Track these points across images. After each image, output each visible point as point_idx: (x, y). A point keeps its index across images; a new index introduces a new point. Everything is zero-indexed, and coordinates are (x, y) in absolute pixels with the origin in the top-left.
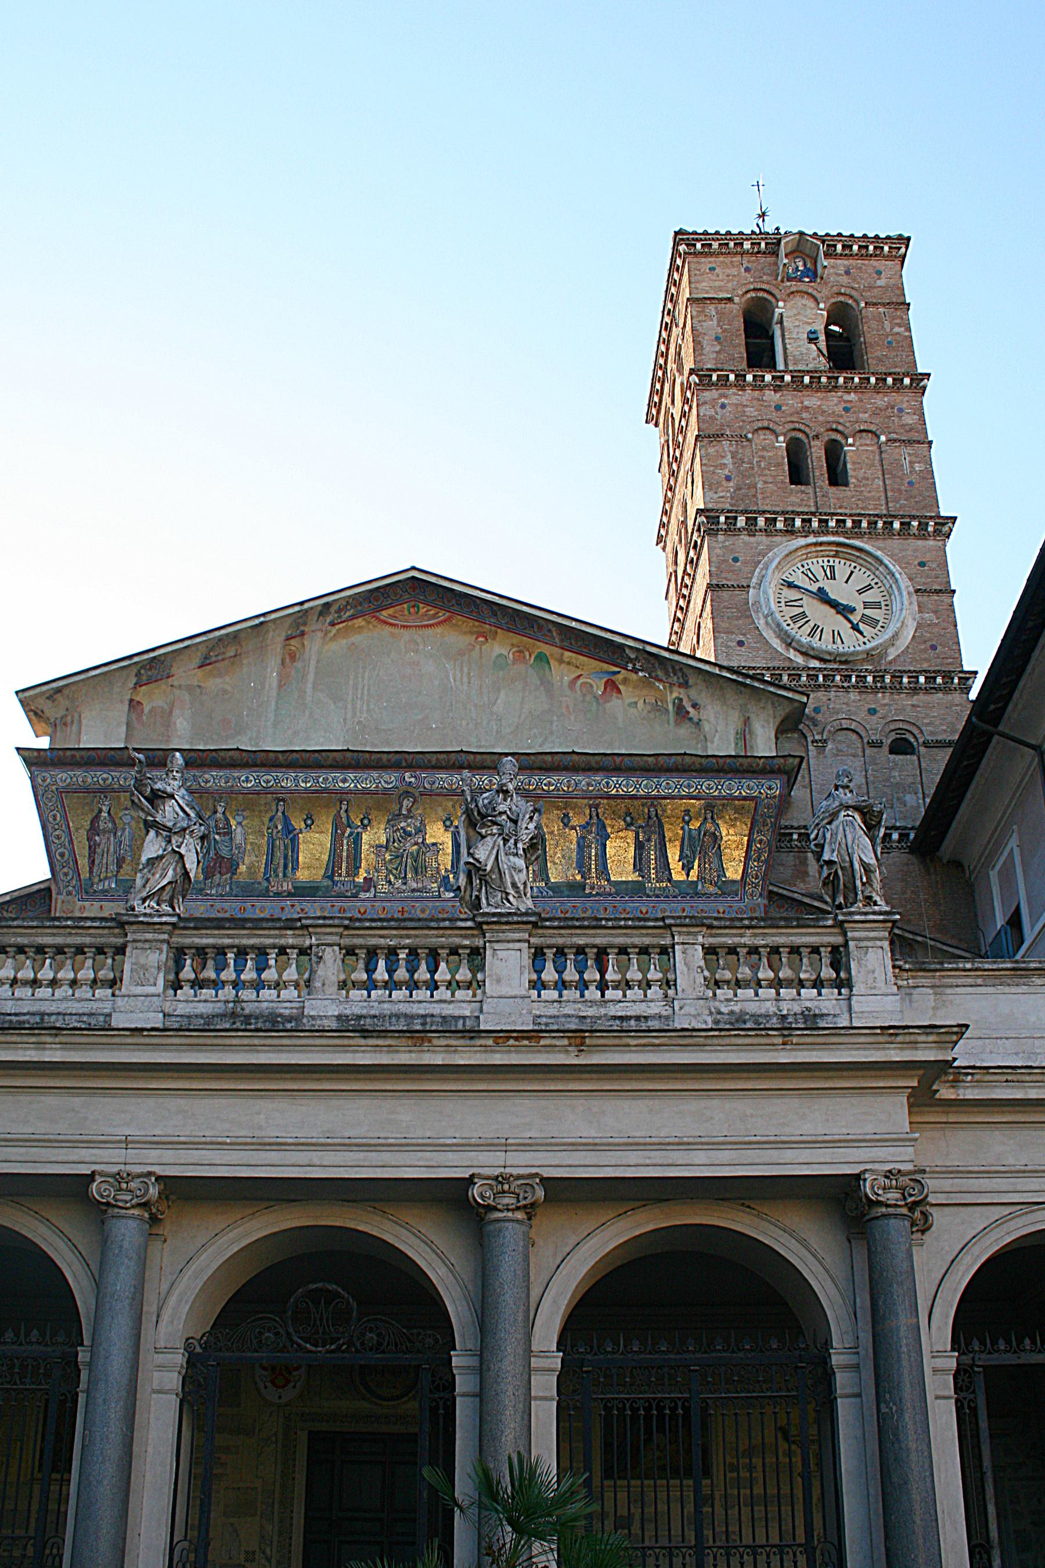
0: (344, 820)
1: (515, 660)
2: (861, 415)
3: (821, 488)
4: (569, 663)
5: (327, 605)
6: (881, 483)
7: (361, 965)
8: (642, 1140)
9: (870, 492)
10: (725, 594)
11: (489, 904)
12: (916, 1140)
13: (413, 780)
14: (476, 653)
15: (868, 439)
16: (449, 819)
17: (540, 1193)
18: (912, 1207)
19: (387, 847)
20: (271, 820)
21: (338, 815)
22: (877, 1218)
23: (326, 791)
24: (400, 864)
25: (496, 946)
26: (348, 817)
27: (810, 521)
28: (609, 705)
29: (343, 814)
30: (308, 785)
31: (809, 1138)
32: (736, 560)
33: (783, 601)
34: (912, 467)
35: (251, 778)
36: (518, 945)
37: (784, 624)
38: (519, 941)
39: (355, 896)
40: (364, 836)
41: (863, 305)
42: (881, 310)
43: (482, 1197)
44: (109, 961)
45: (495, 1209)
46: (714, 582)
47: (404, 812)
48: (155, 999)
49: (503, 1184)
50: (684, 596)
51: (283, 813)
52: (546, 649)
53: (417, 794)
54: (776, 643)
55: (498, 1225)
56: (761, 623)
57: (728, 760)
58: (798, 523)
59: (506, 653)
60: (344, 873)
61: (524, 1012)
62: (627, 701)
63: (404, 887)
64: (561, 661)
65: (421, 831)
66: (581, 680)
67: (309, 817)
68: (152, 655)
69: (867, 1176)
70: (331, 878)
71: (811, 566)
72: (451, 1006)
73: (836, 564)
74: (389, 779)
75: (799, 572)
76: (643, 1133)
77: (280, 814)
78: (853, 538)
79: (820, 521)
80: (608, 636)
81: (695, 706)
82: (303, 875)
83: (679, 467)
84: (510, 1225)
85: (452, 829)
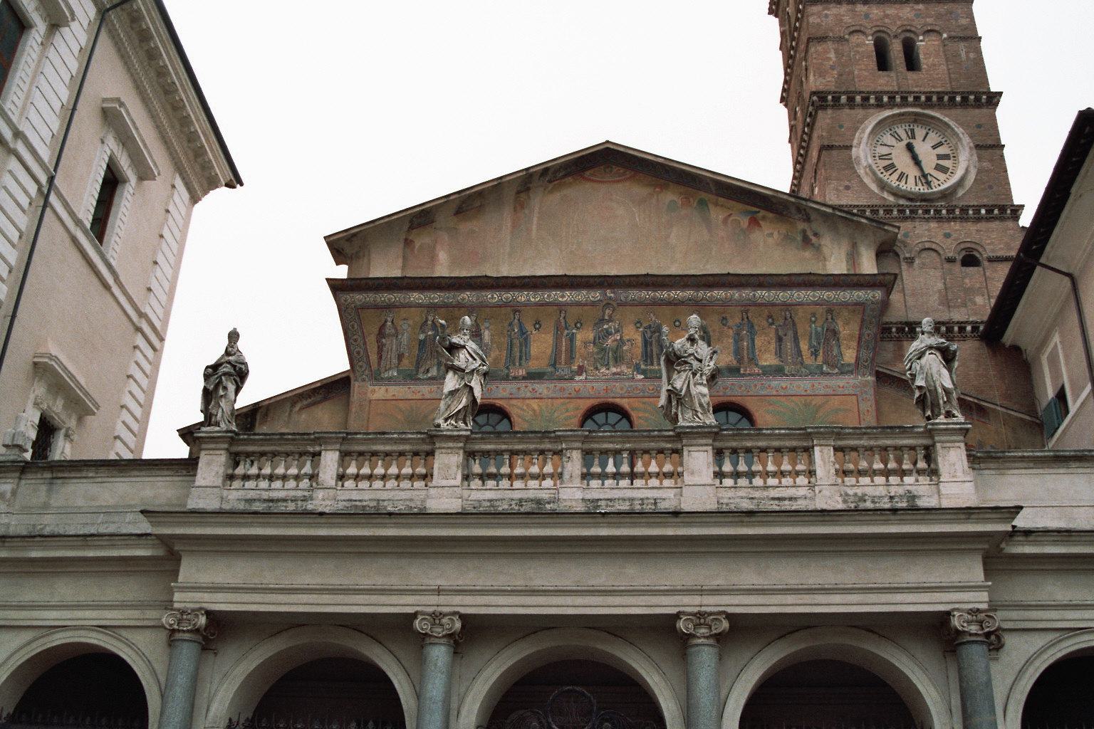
0: (563, 324)
1: (682, 204)
2: (928, 20)
3: (902, 73)
4: (722, 206)
7: (596, 462)
8: (796, 587)
9: (937, 74)
10: (834, 153)
11: (684, 419)
12: (989, 586)
13: (612, 295)
14: (654, 201)
15: (933, 37)
16: (638, 322)
17: (725, 625)
18: (988, 635)
19: (594, 343)
20: (510, 324)
21: (558, 322)
22: (964, 643)
23: (548, 304)
24: (604, 355)
25: (691, 448)
26: (566, 322)
27: (894, 97)
29: (563, 321)
30: (537, 300)
31: (913, 585)
32: (841, 126)
33: (877, 155)
35: (495, 296)
36: (705, 448)
37: (879, 173)
38: (706, 445)
39: (572, 379)
40: (579, 337)
43: (687, 629)
44: (423, 461)
46: (826, 143)
48: (456, 489)
49: (700, 618)
50: (803, 148)
51: (519, 320)
52: (704, 195)
53: (615, 305)
54: (874, 187)
55: (697, 648)
56: (861, 172)
57: (842, 278)
58: (885, 99)
59: (675, 199)
60: (563, 363)
61: (711, 495)
62: (766, 232)
63: (607, 372)
64: (716, 204)
65: (619, 331)
66: (731, 219)
67: (538, 322)
68: (423, 207)
69: (955, 613)
70: (554, 365)
71: (896, 129)
72: (661, 491)
73: (916, 128)
74: (596, 295)
75: (888, 135)
76: (798, 582)
77: (516, 321)
78: (927, 109)
79: (902, 98)
80: (752, 188)
81: (816, 234)
82: (534, 366)
83: (795, 52)
84: (706, 649)
85: (641, 329)
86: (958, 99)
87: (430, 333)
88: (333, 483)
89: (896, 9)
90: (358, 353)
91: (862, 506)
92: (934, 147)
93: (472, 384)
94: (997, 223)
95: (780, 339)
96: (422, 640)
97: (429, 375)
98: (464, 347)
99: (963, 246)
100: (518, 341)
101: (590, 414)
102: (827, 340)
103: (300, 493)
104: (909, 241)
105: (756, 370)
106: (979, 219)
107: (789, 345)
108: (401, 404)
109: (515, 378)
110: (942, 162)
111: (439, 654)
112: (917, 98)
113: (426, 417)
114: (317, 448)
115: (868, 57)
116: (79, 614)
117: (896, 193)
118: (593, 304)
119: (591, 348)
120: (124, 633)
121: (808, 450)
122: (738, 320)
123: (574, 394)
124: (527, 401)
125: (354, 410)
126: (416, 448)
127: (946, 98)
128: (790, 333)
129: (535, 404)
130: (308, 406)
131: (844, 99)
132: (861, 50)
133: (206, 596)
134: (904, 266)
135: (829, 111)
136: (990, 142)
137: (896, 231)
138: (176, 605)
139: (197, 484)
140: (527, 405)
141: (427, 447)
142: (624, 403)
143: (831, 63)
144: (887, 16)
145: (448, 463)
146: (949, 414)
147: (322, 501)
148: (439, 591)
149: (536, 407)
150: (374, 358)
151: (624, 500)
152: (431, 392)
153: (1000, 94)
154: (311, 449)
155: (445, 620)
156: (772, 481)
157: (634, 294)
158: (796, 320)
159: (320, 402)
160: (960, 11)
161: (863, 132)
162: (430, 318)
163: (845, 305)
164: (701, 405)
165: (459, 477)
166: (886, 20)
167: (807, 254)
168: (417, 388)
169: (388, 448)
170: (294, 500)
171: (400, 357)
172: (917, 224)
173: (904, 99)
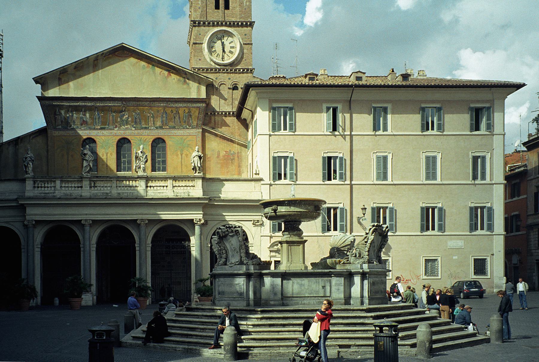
5: (103, 53)
17: (147, 222)
28: (168, 79)
34: (246, 4)
45: (141, 224)
47: (123, 110)
70: (108, 125)
85: (134, 114)
87: (70, 114)
88: (59, 189)
90: (49, 121)
93: (90, 164)
94: (246, 74)
96: (83, 225)
97: (71, 128)
98: (87, 154)
99: (233, 83)
102: (188, 118)
103: (52, 191)
104: (217, 80)
105: (168, 127)
106: (240, 73)
107: (177, 118)
109: (97, 129)
111: (87, 228)
114: (55, 180)
118: (119, 106)
119: (119, 120)
120: (11, 223)
121: (168, 180)
122: (162, 111)
123: (114, 134)
124: (101, 137)
126: (78, 180)
128: (178, 116)
129: (103, 138)
130: (35, 137)
133: (34, 217)
137: (212, 80)
138: (27, 219)
139: (27, 189)
141: (80, 180)
142: (129, 137)
145: (86, 183)
146: (199, 173)
147: (58, 194)
148: (86, 215)
150: (54, 122)
151: (126, 193)
152: (72, 133)
154: (53, 180)
155: (88, 221)
156: (159, 188)
162: (70, 109)
163: (194, 107)
164: (143, 170)
165: (89, 187)
167: (185, 86)
168: (68, 132)
169: (71, 180)
170: (51, 193)
171: (62, 121)
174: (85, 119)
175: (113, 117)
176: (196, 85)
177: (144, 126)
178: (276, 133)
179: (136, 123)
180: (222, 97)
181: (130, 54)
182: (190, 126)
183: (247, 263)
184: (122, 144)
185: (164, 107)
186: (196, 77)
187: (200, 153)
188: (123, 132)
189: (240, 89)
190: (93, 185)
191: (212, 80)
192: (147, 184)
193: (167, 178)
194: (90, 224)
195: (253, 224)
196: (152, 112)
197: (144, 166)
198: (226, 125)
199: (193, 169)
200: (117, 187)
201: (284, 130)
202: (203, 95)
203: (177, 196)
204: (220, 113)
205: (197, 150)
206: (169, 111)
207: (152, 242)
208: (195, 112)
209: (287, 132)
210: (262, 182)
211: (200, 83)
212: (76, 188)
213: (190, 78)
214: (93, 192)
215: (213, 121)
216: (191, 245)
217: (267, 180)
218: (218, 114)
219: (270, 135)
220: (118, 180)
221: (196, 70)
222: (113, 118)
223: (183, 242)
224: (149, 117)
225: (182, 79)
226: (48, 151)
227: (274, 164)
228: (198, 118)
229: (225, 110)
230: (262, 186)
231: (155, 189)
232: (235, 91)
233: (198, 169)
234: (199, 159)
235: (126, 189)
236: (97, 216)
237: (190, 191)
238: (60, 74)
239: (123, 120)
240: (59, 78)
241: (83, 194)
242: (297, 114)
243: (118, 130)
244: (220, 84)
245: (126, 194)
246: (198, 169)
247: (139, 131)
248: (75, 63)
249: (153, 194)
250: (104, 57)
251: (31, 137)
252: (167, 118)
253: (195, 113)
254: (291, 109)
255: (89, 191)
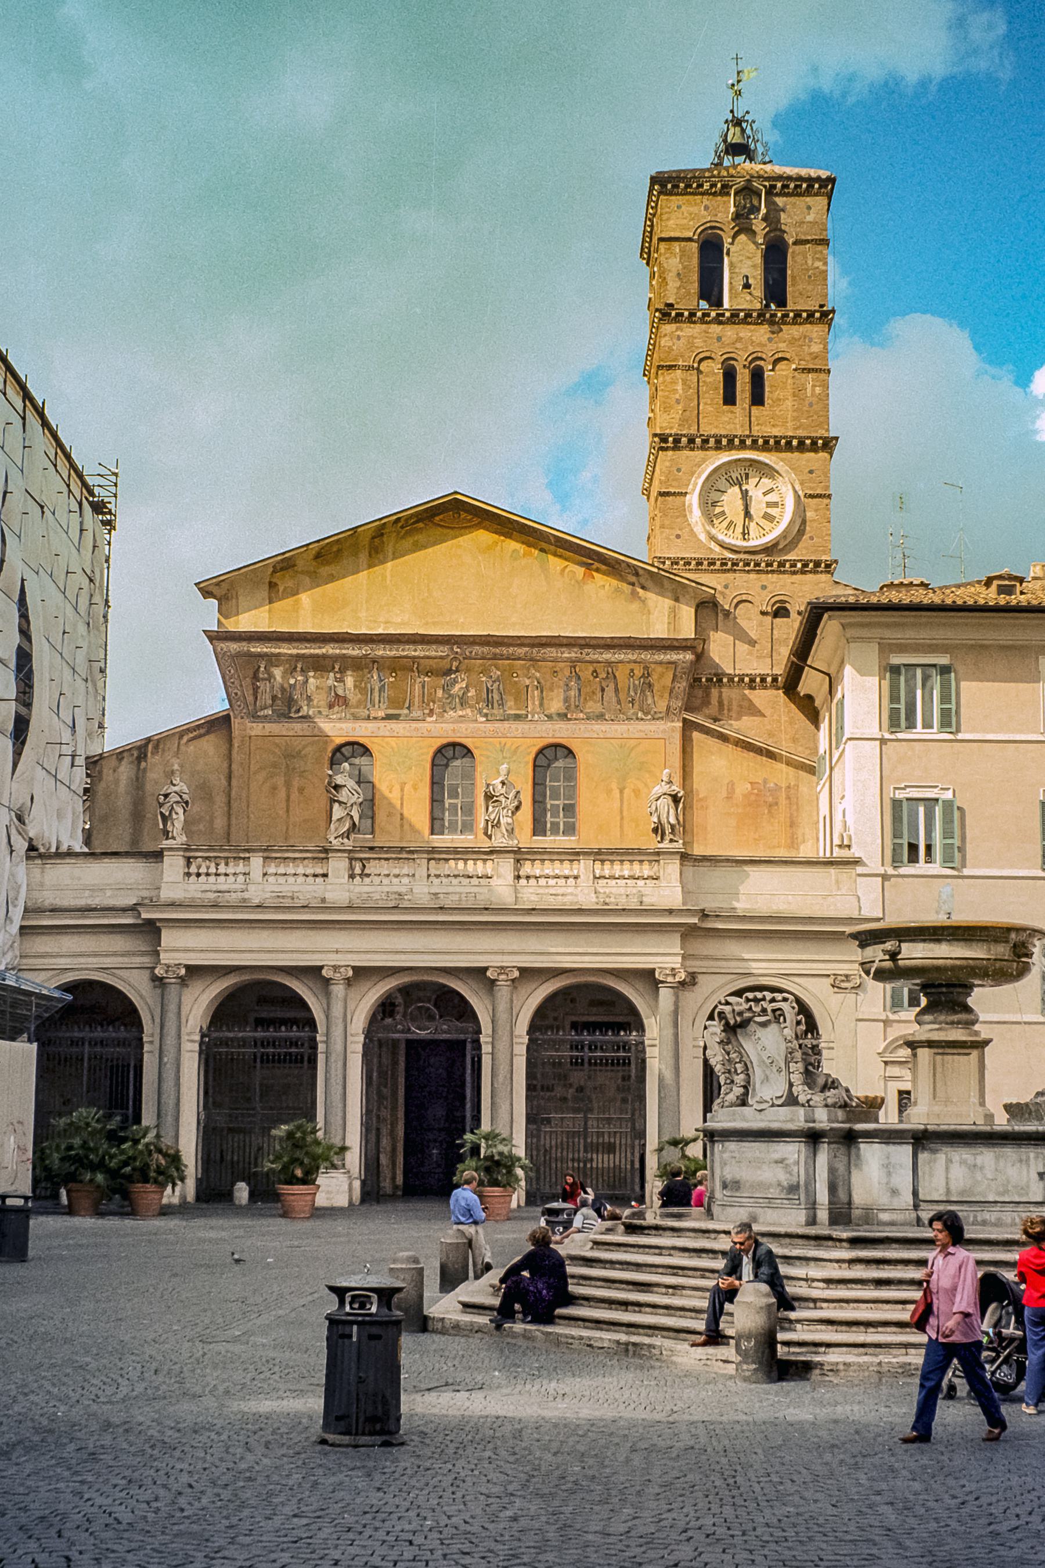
4: (560, 556)
6: (789, 403)
15: (781, 366)
32: (679, 470)
33: (710, 502)
41: (791, 241)
42: (808, 246)
54: (703, 537)
70: (409, 708)
86: (795, 443)
87: (299, 678)
89: (751, 331)
91: (607, 900)
92: (765, 494)
95: (603, 690)
96: (327, 982)
97: (300, 714)
100: (377, 689)
101: (440, 751)
104: (727, 591)
106: (794, 573)
108: (277, 740)
109: (375, 718)
110: (769, 510)
111: (338, 990)
112: (755, 442)
113: (300, 751)
115: (717, 389)
116: (82, 960)
117: (722, 545)
118: (441, 657)
121: (579, 860)
122: (568, 674)
125: (236, 745)
127: (783, 442)
128: (612, 686)
129: (393, 742)
131: (684, 440)
132: (708, 380)
134: (721, 616)
135: (670, 453)
136: (819, 492)
137: (713, 592)
138: (162, 962)
140: (387, 743)
143: (677, 396)
144: (739, 339)
146: (671, 841)
149: (395, 745)
153: (837, 438)
155: (342, 970)
156: (551, 882)
157: (477, 649)
158: (617, 674)
159: (204, 735)
160: (815, 335)
161: (699, 477)
163: (661, 663)
165: (346, 877)
166: (738, 345)
167: (635, 606)
171: (274, 698)
172: (737, 575)
173: (743, 442)
174: (340, 692)
175: (423, 687)
176: (667, 603)
177: (513, 712)
178: (900, 736)
179: (489, 702)
180: (741, 635)
181: (476, 520)
182: (646, 714)
183: (808, 1101)
184: (448, 760)
185: (573, 663)
186: (666, 582)
187: (674, 788)
188: (451, 726)
189: (793, 615)
190: (358, 871)
191: (713, 592)
192: (517, 869)
193: (578, 854)
194: (348, 979)
195: (833, 986)
196: (538, 675)
197: (510, 820)
198: (754, 711)
199: (655, 830)
200: (429, 876)
201: (924, 727)
202: (687, 630)
203: (607, 904)
204: (736, 679)
205: (665, 779)
206: (586, 673)
207: (532, 1029)
208: (662, 675)
209: (934, 733)
210: (860, 870)
211: (677, 600)
212: (311, 879)
213: (649, 584)
214: (358, 889)
215: (714, 701)
216: (647, 1042)
217: (874, 864)
218: (731, 680)
219: (883, 741)
220: (434, 859)
221: (668, 562)
222: (423, 687)
223: (622, 1033)
224: (527, 687)
225: (626, 588)
226: (229, 778)
227: (897, 819)
228: (671, 692)
229: (749, 672)
230: (859, 879)
231: (540, 883)
232: (778, 620)
233: (668, 830)
234: (672, 804)
235: (455, 881)
236: (369, 956)
237: (646, 891)
238: (274, 572)
239: (450, 695)
240: (270, 583)
241: (329, 896)
242: (963, 684)
243: (436, 721)
244: (735, 601)
245: (456, 898)
246: (668, 830)
247: (498, 725)
248: (316, 545)
249: (534, 898)
250: (402, 527)
251: (185, 739)
252: (579, 690)
253: (663, 679)
254: (945, 670)
255: (346, 887)
